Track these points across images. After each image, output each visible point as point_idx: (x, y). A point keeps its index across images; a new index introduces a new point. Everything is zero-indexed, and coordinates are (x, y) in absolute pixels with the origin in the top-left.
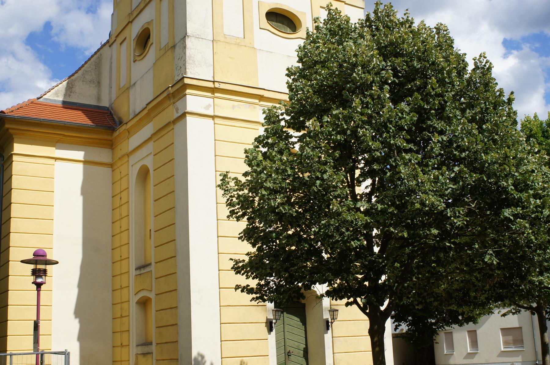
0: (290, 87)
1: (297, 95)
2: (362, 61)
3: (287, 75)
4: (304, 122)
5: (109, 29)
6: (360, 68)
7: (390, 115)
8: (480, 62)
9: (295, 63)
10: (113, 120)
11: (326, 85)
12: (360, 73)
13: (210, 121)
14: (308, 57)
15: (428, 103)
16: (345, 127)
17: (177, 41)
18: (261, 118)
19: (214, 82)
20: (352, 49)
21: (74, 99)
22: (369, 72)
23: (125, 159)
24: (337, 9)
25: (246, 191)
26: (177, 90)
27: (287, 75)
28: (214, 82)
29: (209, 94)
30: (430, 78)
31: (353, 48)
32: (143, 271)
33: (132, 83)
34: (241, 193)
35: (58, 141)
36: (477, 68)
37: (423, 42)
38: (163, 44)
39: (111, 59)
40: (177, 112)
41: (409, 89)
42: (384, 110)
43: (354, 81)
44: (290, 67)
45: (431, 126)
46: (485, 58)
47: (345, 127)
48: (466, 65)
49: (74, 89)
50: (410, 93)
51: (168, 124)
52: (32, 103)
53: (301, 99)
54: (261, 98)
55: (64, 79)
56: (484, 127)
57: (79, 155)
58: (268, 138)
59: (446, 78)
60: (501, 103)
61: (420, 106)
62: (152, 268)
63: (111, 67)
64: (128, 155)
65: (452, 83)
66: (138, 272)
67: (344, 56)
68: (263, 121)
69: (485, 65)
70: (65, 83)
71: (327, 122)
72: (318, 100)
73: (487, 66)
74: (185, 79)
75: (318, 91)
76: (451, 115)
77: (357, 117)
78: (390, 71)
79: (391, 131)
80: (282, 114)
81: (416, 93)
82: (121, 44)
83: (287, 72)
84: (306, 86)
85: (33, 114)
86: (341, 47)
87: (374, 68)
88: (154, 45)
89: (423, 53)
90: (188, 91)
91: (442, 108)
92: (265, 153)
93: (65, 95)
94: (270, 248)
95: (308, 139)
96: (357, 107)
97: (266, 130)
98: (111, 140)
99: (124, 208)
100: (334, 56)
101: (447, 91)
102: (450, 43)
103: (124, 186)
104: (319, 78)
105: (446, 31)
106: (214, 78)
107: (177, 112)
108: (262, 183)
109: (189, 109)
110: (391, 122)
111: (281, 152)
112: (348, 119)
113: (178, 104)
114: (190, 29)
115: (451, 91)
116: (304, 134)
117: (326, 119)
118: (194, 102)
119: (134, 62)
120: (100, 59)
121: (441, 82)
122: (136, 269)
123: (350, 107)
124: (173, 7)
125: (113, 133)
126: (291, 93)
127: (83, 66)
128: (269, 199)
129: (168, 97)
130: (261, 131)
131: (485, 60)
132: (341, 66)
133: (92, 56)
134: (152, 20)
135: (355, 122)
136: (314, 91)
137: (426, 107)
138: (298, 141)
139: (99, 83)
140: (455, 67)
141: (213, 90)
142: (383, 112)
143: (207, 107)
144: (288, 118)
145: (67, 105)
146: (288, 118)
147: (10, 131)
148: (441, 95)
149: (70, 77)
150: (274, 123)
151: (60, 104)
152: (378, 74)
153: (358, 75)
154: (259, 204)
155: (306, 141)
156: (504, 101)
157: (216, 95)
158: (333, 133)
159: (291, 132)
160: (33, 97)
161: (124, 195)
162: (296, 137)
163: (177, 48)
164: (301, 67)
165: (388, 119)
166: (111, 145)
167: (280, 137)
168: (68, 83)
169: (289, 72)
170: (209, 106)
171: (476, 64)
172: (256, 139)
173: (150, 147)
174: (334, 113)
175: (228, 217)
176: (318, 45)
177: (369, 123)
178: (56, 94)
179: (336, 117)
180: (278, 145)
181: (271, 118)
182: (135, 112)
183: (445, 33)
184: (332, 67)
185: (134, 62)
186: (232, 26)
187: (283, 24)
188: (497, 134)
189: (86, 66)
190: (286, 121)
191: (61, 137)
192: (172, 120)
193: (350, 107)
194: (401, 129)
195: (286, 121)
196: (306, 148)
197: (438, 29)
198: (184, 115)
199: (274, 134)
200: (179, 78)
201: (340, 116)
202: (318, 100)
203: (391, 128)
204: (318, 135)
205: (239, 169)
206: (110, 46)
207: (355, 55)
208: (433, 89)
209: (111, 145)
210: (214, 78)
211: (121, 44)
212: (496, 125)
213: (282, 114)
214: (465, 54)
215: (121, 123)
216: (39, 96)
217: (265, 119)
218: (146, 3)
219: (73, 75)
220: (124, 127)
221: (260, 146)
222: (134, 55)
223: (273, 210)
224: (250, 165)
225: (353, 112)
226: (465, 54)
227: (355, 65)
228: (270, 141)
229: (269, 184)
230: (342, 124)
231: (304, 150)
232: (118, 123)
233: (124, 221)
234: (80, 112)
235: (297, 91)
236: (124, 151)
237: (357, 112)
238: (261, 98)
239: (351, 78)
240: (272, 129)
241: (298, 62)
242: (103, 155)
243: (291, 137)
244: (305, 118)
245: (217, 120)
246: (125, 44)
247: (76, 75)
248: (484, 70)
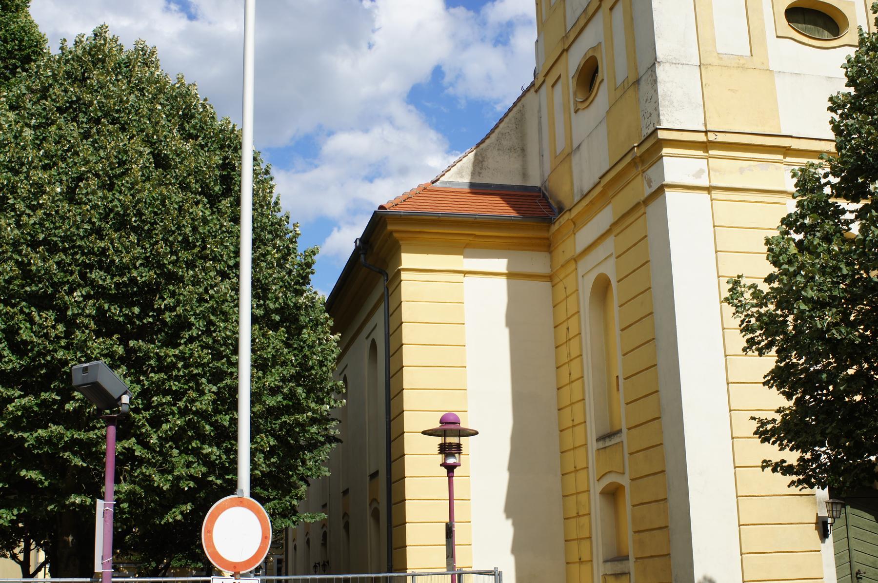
0: (836, 128)
1: (850, 141)
3: (831, 109)
4: (864, 185)
5: (533, 65)
9: (841, 87)
10: (549, 206)
13: (704, 195)
17: (642, 71)
18: (790, 185)
19: (706, 132)
21: (486, 179)
23: (572, 266)
25: (771, 307)
26: (648, 150)
27: (831, 109)
28: (706, 132)
29: (700, 153)
32: (608, 443)
33: (575, 146)
34: (763, 310)
35: (467, 246)
38: (620, 79)
39: (539, 111)
40: (650, 186)
44: (835, 94)
49: (485, 164)
51: (638, 204)
52: (424, 189)
53: (858, 146)
54: (786, 151)
55: (469, 150)
57: (500, 264)
58: (803, 216)
62: (624, 437)
63: (540, 123)
64: (576, 259)
66: (601, 445)
68: (794, 190)
70: (471, 156)
74: (659, 132)
82: (553, 86)
83: (830, 104)
84: (866, 124)
85: (426, 207)
90: (665, 151)
92: (801, 241)
93: (473, 174)
94: (818, 401)
97: (800, 204)
98: (548, 239)
99: (574, 343)
103: (572, 310)
106: (705, 126)
107: (650, 186)
108: (798, 291)
109: (669, 179)
111: (827, 238)
113: (651, 173)
116: (866, 205)
118: (676, 167)
119: (576, 112)
120: (522, 113)
122: (598, 440)
124: (632, 19)
125: (549, 227)
126: (839, 139)
127: (497, 126)
128: (812, 317)
129: (634, 163)
130: (791, 207)
133: (510, 110)
134: (600, 43)
139: (523, 150)
141: (705, 146)
143: (698, 174)
144: (835, 180)
145: (477, 189)
146: (835, 180)
147: (396, 235)
149: (478, 145)
150: (812, 191)
151: (466, 188)
154: (795, 327)
155: (872, 216)
157: (712, 152)
159: (843, 203)
160: (426, 180)
161: (573, 323)
162: (851, 212)
163: (642, 83)
164: (853, 93)
166: (548, 246)
168: (476, 155)
169: (834, 103)
170: (701, 171)
172: (783, 221)
173: (609, 246)
175: (744, 350)
178: (460, 173)
180: (822, 227)
181: (807, 184)
182: (582, 191)
185: (576, 112)
187: (815, 24)
189: (501, 126)
190: (833, 186)
191: (471, 239)
192: (642, 198)
195: (833, 186)
196: (872, 228)
198: (661, 189)
199: (814, 210)
200: (649, 131)
205: (758, 270)
206: (536, 91)
209: (548, 246)
210: (705, 126)
211: (553, 86)
213: (826, 176)
215: (561, 210)
216: (434, 178)
217: (796, 185)
218: (588, 17)
219: (483, 141)
220: (566, 216)
221: (791, 232)
222: (576, 102)
223: (819, 335)
224: (775, 263)
228: (807, 221)
229: (810, 293)
231: (867, 231)
232: (556, 211)
233: (575, 364)
234: (497, 198)
235: (849, 134)
236: (569, 255)
238: (786, 151)
240: (810, 202)
241: (848, 85)
242: (536, 262)
243: (843, 212)
244: (866, 179)
245: (716, 194)
246: (559, 86)
247: (488, 141)
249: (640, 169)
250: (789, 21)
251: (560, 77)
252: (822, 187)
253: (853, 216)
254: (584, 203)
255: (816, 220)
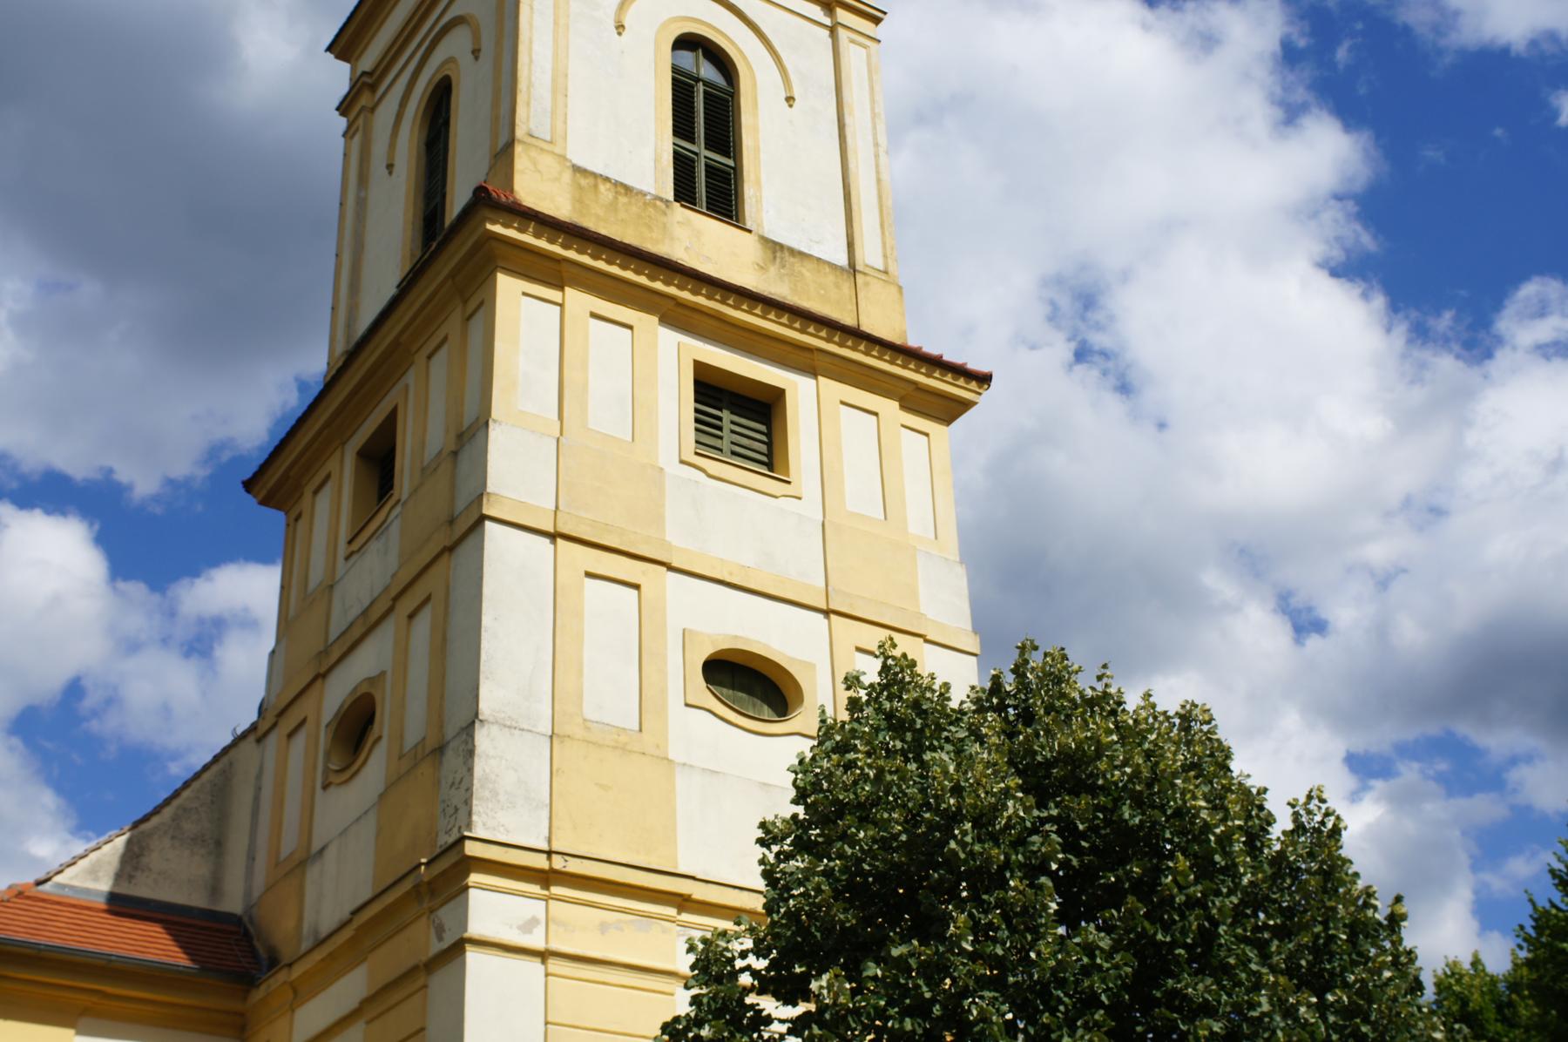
0: (768, 875)
1: (787, 900)
2: (975, 806)
3: (761, 842)
4: (805, 979)
5: (260, 693)
6: (968, 826)
7: (1059, 962)
8: (1309, 812)
9: (784, 808)
11: (869, 873)
12: (968, 839)
13: (535, 966)
14: (822, 790)
15: (1166, 929)
16: (928, 995)
17: (450, 731)
18: (684, 963)
19: (549, 853)
20: (945, 772)
22: (995, 839)
24: (904, 656)
26: (443, 873)
27: (761, 842)
28: (549, 853)
29: (535, 889)
30: (1171, 856)
31: (952, 768)
36: (1299, 828)
37: (1148, 755)
38: (411, 740)
39: (259, 776)
40: (440, 939)
41: (1108, 887)
42: (1041, 945)
43: (951, 861)
44: (770, 818)
45: (1175, 993)
46: (1323, 801)
47: (928, 995)
48: (1270, 820)
50: (1114, 896)
51: (413, 971)
53: (799, 910)
54: (684, 903)
56: (1330, 998)
58: (699, 1022)
59: (1214, 852)
60: (1376, 929)
61: (1143, 934)
65: (1231, 870)
67: (923, 791)
68: (687, 971)
69: (1323, 823)
71: (875, 978)
72: (846, 918)
73: (1330, 825)
75: (846, 889)
76: (1232, 961)
77: (961, 968)
78: (1054, 836)
79: (1062, 1008)
80: (743, 955)
81: (1130, 899)
82: (290, 735)
83: (760, 834)
84: (815, 874)
86: (912, 766)
87: (1008, 826)
88: (383, 744)
89: (1150, 785)
90: (474, 878)
91: (1207, 937)
95: (816, 1030)
96: (961, 937)
97: (695, 1001)
100: (895, 789)
101: (1218, 893)
102: (1220, 757)
104: (849, 851)
105: (1209, 722)
106: (549, 841)
107: (440, 939)
109: (475, 928)
110: (1061, 984)
112: (934, 970)
113: (445, 914)
114: (485, 707)
115: (1231, 892)
116: (808, 1013)
117: (873, 970)
118: (490, 909)
119: (325, 787)
121: (1204, 868)
123: (942, 938)
124: (444, 639)
126: (773, 894)
129: (417, 892)
130: (680, 1003)
131: (1324, 806)
132: (912, 821)
134: (383, 673)
135: (954, 980)
136: (835, 890)
137: (1159, 936)
138: (790, 1032)
140: (1240, 827)
141: (546, 878)
142: (1039, 954)
143: (528, 926)
144: (761, 964)
146: (761, 964)
148: (1202, 904)
150: (718, 979)
152: (1020, 842)
153: (963, 844)
156: (1379, 924)
157: (555, 890)
158: (893, 1011)
159: (768, 1005)
162: (782, 1021)
163: (449, 753)
164: (801, 817)
165: (1054, 971)
167: (736, 1024)
169: (767, 832)
170: (533, 922)
171: (1296, 816)
174: (895, 952)
176: (852, 756)
177: (997, 983)
179: (901, 964)
181: (711, 966)
183: (1205, 728)
184: (890, 820)
185: (325, 787)
186: (608, 695)
187: (750, 692)
188: (1366, 1021)
190: (755, 974)
192: (424, 959)
193: (942, 938)
194: (1091, 1001)
195: (755, 974)
197: (1186, 718)
198: (457, 948)
200: (451, 840)
201: (913, 962)
202: (846, 918)
203: (1060, 1001)
204: (844, 1018)
206: (259, 741)
207: (957, 790)
208: (1181, 888)
210: (549, 841)
212: (1364, 992)
213: (743, 955)
214: (1265, 790)
217: (693, 968)
222: (326, 771)
225: (951, 951)
226: (1265, 790)
227: (954, 818)
230: (917, 987)
235: (787, 888)
237: (963, 952)
238: (684, 903)
239: (942, 854)
240: (714, 999)
241: (795, 802)
243: (769, 1020)
244: (810, 968)
245: (555, 965)
246: (300, 740)
248: (1320, 838)
249: (426, 905)
250: (707, 680)
251: (303, 722)
252: (735, 974)
253: (783, 1028)
254: (318, 956)
255: (720, 1031)
